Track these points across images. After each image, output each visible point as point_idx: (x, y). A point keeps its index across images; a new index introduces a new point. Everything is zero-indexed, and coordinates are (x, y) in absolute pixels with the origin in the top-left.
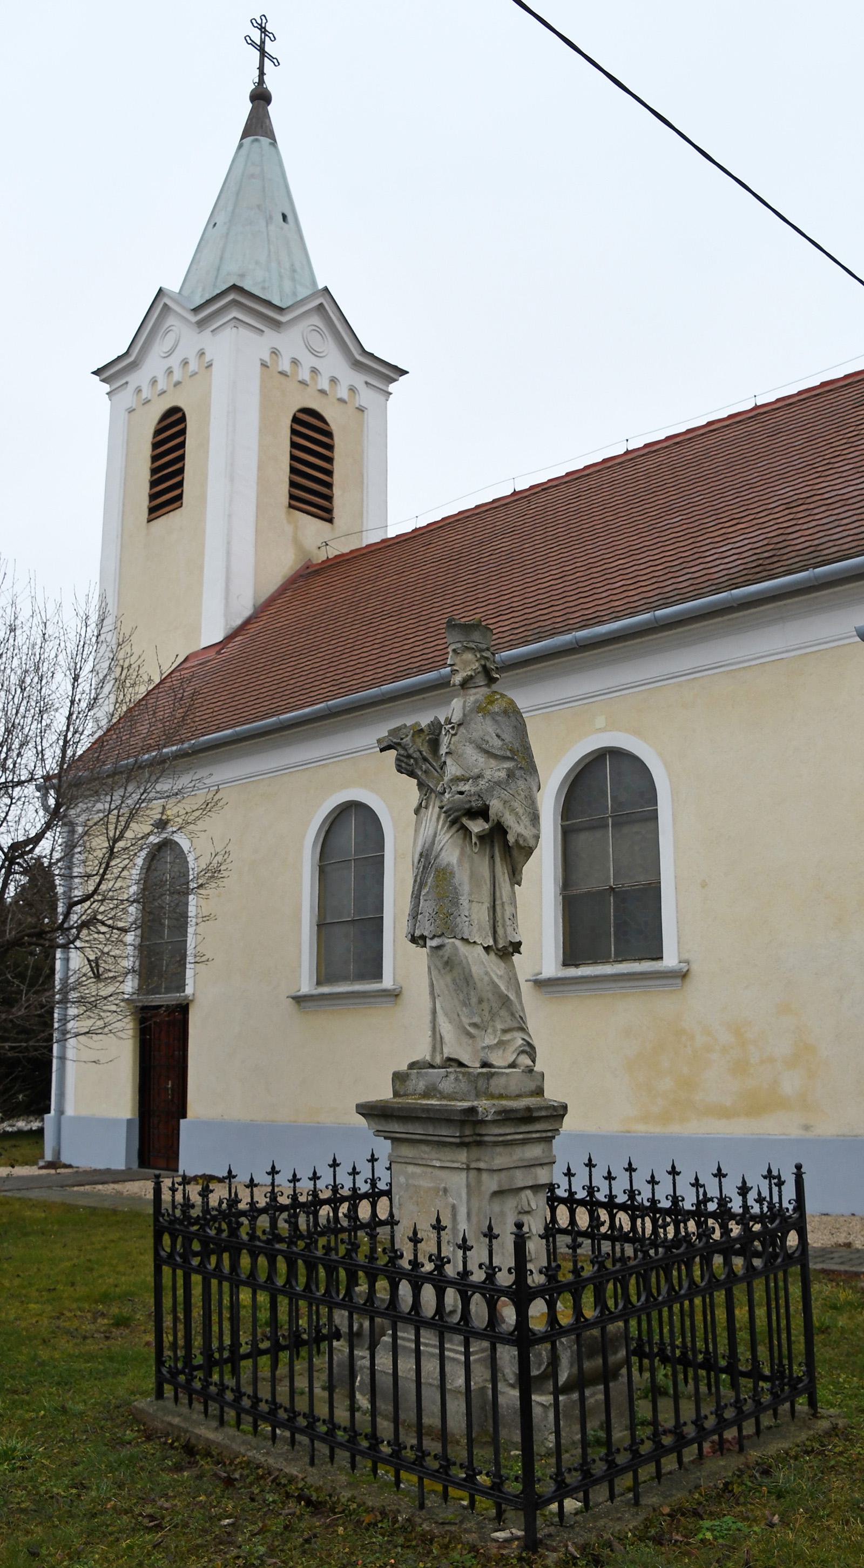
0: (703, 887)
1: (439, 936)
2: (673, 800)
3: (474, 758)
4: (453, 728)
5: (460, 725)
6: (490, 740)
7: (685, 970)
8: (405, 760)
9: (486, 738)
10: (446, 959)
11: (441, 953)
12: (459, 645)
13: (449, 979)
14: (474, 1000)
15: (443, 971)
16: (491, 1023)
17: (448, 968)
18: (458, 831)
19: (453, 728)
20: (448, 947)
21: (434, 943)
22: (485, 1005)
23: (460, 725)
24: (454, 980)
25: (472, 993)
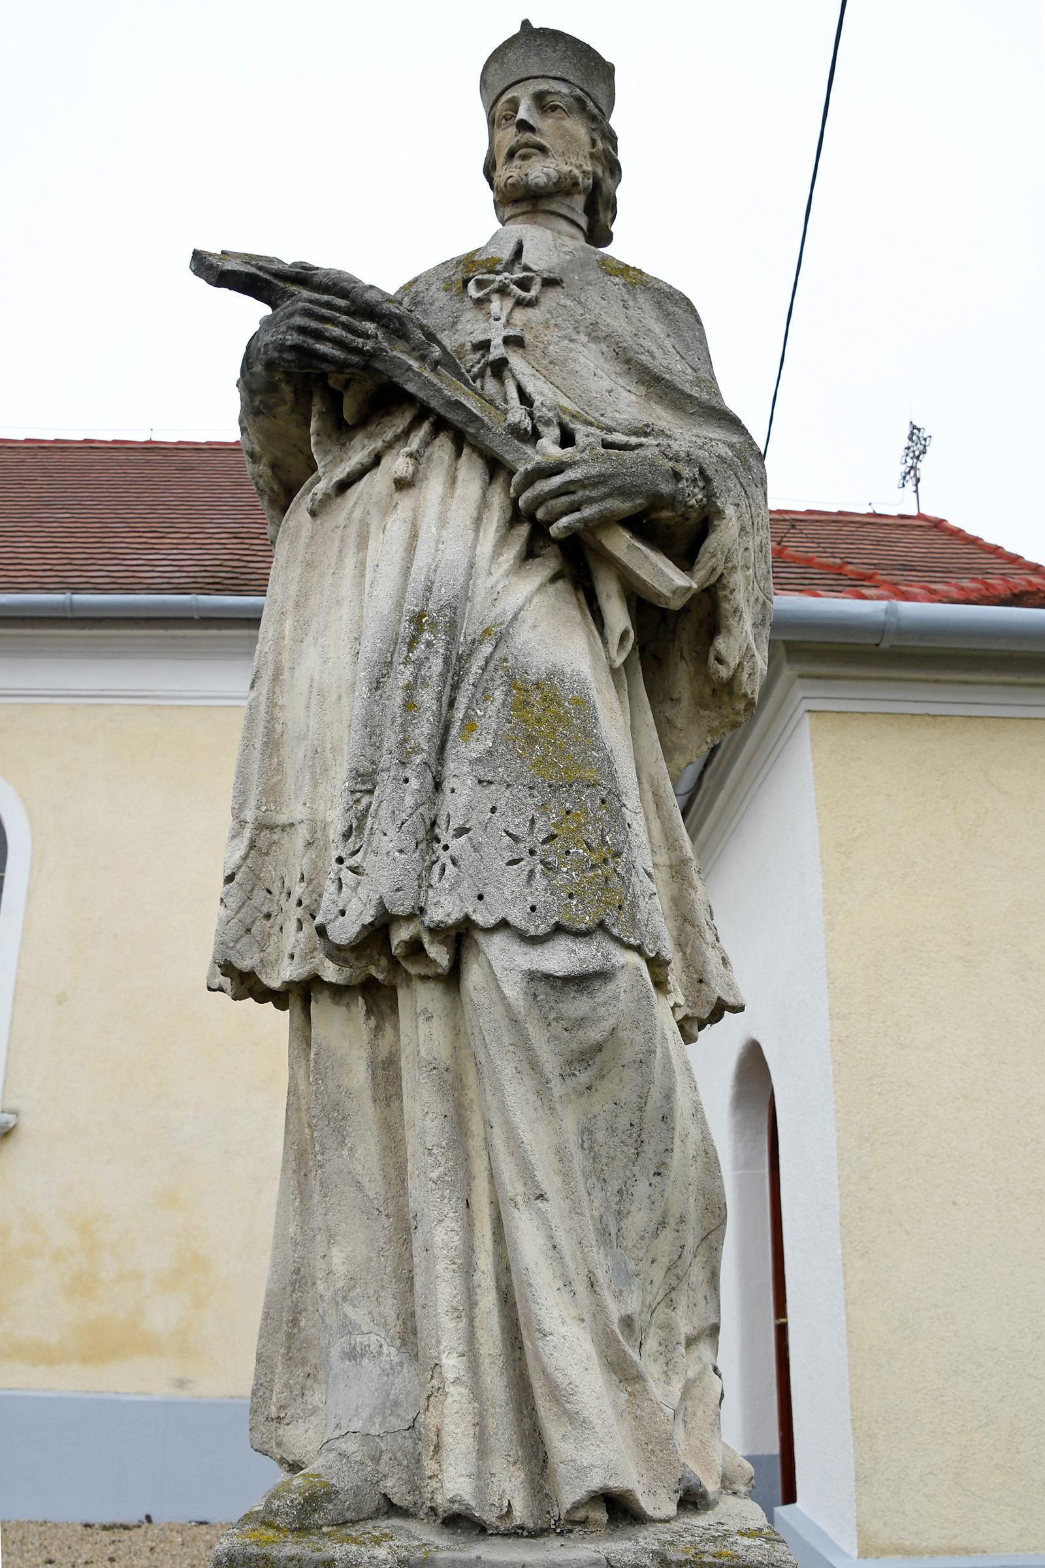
0: (60, 1003)
1: (578, 934)
2: (32, 868)
3: (606, 383)
4: (524, 284)
5: (550, 283)
6: (658, 353)
7: (11, 1125)
8: (344, 318)
9: (647, 343)
10: (594, 1035)
11: (577, 1005)
12: (564, 89)
13: (570, 1125)
14: (639, 1219)
15: (557, 1088)
16: (661, 1315)
17: (583, 1078)
18: (554, 579)
19: (524, 284)
20: (622, 982)
21: (560, 958)
22: (665, 1244)
23: (550, 283)
24: (587, 1132)
25: (641, 1189)
